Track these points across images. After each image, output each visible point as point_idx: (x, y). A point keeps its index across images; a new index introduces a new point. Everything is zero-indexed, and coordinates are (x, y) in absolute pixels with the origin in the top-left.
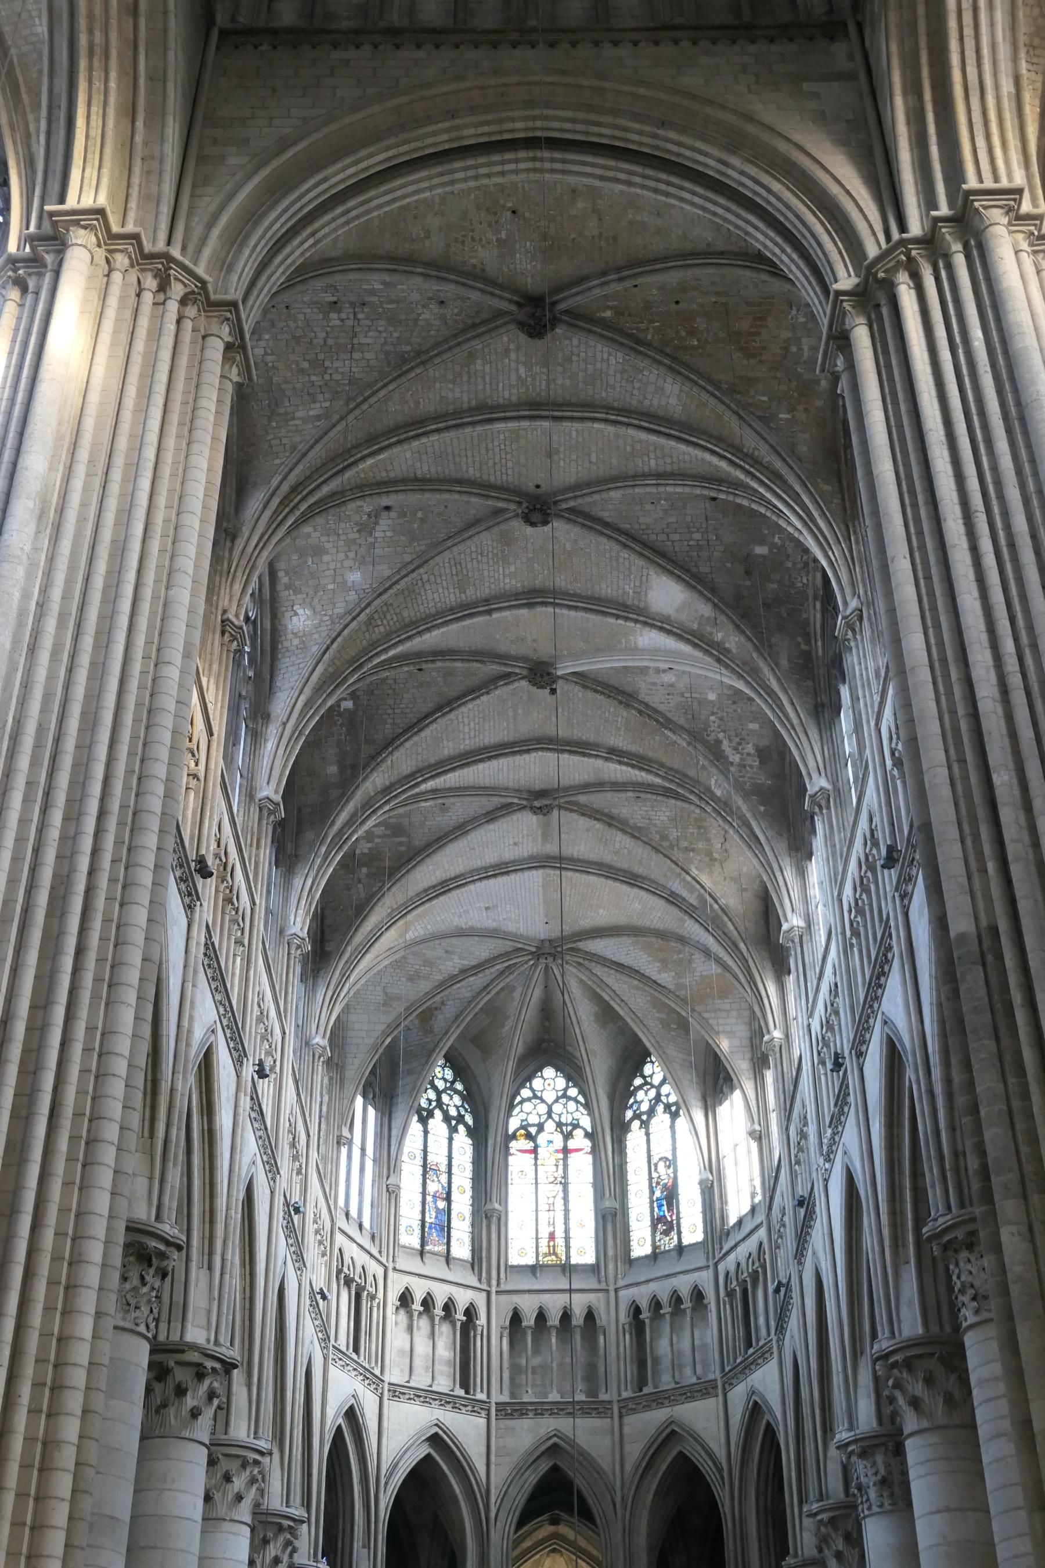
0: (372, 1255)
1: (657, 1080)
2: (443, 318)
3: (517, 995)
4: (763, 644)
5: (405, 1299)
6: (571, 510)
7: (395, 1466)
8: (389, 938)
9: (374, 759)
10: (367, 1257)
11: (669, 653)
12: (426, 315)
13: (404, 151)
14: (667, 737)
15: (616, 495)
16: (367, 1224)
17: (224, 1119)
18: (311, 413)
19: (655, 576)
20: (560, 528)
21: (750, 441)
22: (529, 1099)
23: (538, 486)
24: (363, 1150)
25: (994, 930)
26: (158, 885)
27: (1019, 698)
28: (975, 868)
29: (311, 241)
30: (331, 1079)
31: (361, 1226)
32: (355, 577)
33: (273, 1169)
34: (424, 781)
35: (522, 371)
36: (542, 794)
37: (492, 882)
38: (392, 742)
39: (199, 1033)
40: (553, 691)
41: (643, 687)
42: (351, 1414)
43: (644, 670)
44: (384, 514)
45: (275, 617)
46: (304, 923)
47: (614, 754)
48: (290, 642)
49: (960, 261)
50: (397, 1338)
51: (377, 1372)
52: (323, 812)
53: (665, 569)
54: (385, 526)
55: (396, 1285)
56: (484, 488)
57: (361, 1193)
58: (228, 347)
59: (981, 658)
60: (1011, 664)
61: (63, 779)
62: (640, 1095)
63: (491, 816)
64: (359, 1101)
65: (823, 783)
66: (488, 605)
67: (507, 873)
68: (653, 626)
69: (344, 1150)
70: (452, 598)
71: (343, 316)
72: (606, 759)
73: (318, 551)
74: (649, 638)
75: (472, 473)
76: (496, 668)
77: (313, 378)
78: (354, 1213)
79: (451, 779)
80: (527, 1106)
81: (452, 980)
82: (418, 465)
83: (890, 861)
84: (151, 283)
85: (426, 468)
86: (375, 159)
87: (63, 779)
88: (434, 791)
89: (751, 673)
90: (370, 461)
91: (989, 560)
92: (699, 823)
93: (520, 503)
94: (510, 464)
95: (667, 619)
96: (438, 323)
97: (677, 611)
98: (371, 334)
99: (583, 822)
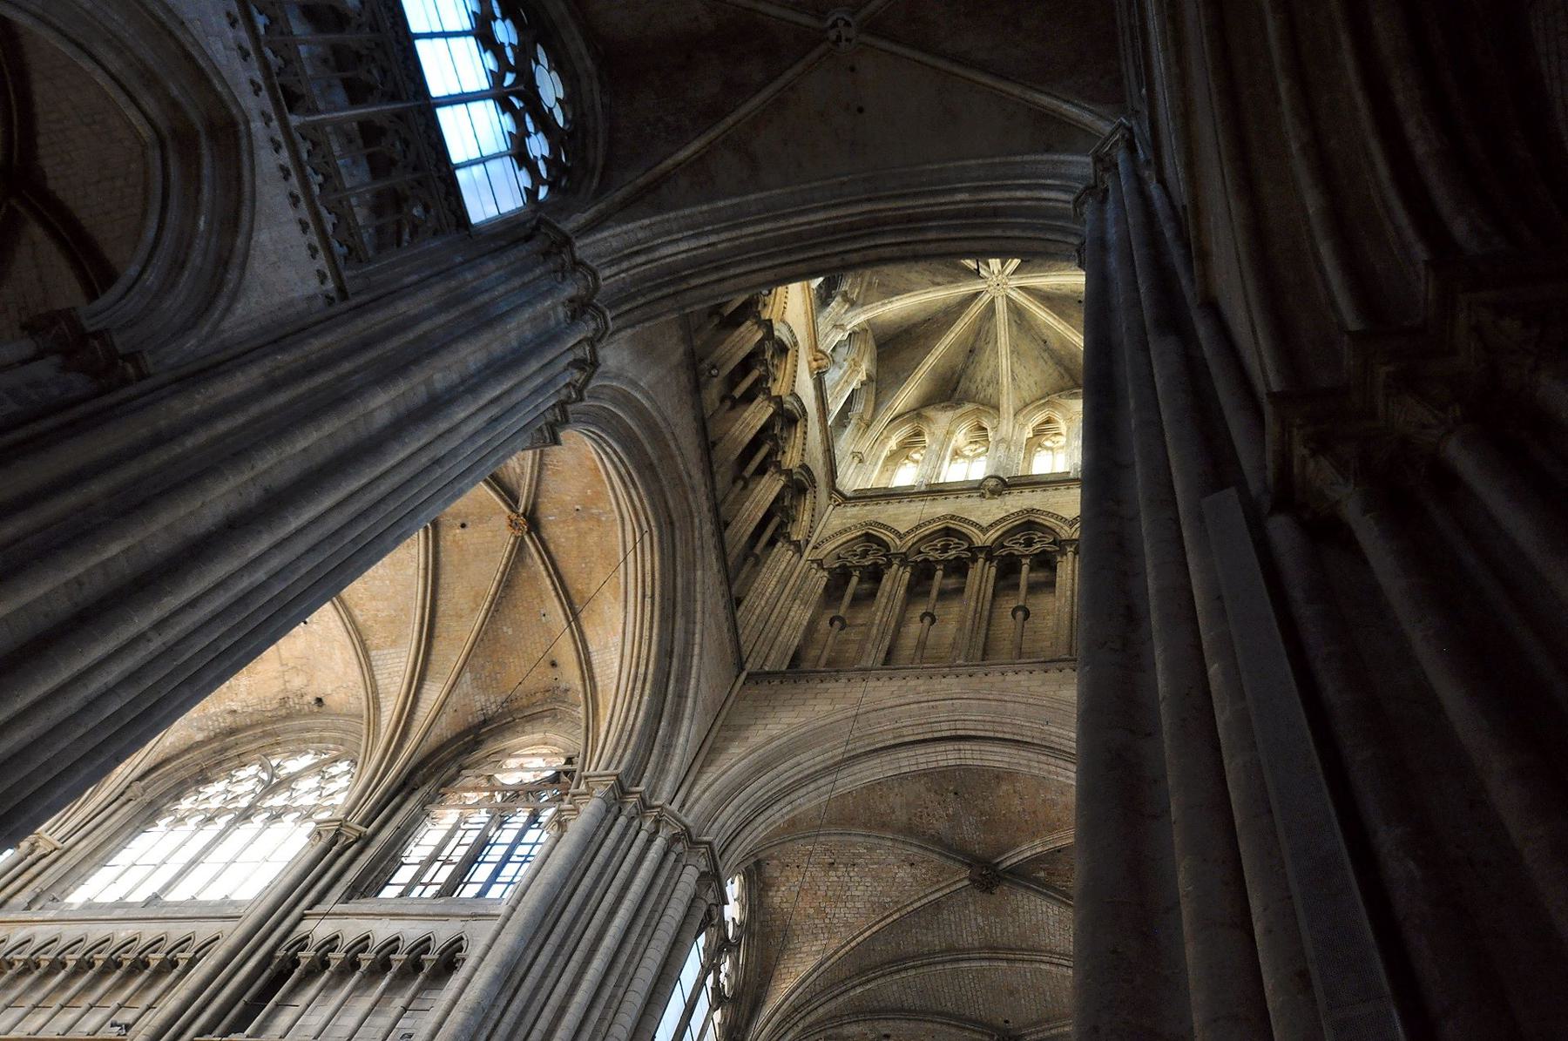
2: (914, 877)
12: (901, 874)
18: (814, 949)
23: (1007, 1022)
29: (789, 808)
35: (980, 919)
58: (703, 875)
71: (839, 874)
77: (816, 921)
82: (904, 997)
90: (859, 990)
94: (980, 1001)
96: (911, 880)
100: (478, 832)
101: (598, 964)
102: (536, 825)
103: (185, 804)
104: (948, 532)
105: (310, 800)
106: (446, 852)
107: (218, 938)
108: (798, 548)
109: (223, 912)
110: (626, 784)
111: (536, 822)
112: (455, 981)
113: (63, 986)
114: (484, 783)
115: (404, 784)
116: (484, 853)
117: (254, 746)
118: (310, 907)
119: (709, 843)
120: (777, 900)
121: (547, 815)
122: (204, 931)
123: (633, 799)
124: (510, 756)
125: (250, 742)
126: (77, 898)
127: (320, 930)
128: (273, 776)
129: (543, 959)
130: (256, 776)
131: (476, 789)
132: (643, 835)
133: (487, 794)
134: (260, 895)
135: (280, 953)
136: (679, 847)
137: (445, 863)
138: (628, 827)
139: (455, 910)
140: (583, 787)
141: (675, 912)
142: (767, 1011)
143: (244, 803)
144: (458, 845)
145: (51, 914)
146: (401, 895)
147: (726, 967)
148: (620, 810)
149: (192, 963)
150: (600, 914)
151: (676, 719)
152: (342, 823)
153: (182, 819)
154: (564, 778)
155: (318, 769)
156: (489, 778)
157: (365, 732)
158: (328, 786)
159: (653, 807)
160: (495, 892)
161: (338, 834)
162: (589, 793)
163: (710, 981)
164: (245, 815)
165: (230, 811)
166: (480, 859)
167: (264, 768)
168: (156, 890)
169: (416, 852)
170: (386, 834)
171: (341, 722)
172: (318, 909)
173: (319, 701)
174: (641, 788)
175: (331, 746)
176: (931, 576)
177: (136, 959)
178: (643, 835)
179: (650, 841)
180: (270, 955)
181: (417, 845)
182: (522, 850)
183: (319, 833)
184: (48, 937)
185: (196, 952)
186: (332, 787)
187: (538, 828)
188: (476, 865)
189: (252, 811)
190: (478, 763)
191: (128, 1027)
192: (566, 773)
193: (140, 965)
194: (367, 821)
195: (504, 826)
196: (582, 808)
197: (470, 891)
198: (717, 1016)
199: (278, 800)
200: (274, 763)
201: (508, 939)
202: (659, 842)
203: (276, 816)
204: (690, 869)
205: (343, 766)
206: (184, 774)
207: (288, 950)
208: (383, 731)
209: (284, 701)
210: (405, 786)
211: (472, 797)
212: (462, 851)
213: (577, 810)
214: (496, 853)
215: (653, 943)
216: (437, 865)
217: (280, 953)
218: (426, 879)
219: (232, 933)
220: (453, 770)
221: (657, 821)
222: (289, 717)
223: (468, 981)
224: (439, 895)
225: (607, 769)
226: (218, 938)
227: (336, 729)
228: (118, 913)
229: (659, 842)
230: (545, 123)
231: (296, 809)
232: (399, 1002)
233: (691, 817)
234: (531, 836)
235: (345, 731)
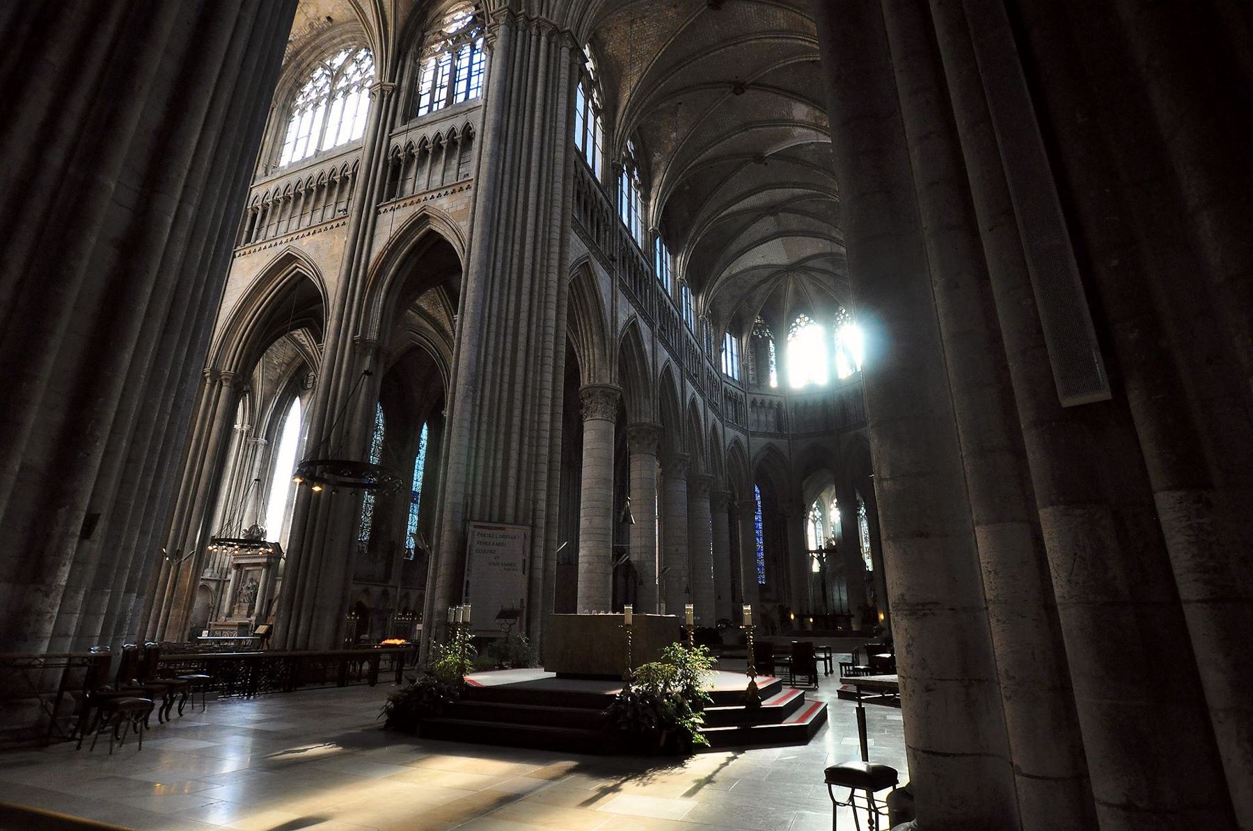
0: (739, 389)
1: (844, 311)
2: (678, 13)
3: (783, 288)
5: (754, 403)
6: (752, 84)
7: (755, 459)
8: (725, 274)
10: (737, 390)
14: (816, 173)
16: (736, 378)
17: (648, 347)
19: (793, 104)
20: (749, 93)
22: (795, 326)
23: (737, 77)
24: (732, 353)
30: (715, 331)
31: (734, 379)
33: (680, 364)
34: (723, 212)
36: (772, 207)
37: (761, 246)
39: (622, 318)
40: (766, 164)
42: (736, 442)
44: (679, 106)
46: (683, 274)
47: (796, 185)
50: (752, 416)
51: (746, 428)
53: (800, 101)
55: (750, 398)
57: (732, 367)
58: (571, 50)
62: (838, 319)
63: (754, 221)
64: (728, 335)
67: (766, 242)
68: (797, 126)
69: (723, 354)
72: (793, 188)
74: (798, 131)
78: (730, 375)
79: (734, 208)
80: (794, 329)
81: (755, 287)
88: (728, 215)
93: (731, 87)
95: (802, 121)
96: (676, 16)
97: (807, 116)
98: (651, 29)
99: (791, 216)
100: (449, 65)
101: (538, 114)
102: (476, 52)
103: (300, 101)
105: (357, 78)
106: (439, 82)
107: (358, 160)
109: (353, 148)
110: (514, 11)
111: (475, 49)
112: (476, 144)
113: (306, 203)
114: (440, 38)
115: (399, 52)
116: (457, 76)
117: (312, 57)
118: (391, 132)
119: (569, 31)
120: (610, 51)
121: (480, 43)
122: (351, 161)
123: (521, 19)
124: (445, 15)
125: (309, 56)
126: (284, 162)
128: (331, 71)
129: (512, 121)
130: (323, 73)
131: (437, 41)
132: (534, 38)
133: (443, 42)
134: (364, 134)
135: (390, 158)
136: (554, 39)
137: (441, 87)
138: (524, 36)
139: (458, 110)
140: (492, 21)
141: (564, 74)
142: (621, 109)
143: (327, 90)
144: (443, 76)
145: (278, 175)
146: (429, 111)
147: (595, 95)
148: (517, 28)
149: (354, 175)
150: (529, 89)
152: (381, 84)
153: (304, 109)
154: (479, 19)
155: (351, 58)
156: (440, 32)
157: (364, 29)
158: (362, 66)
159: (533, 20)
160: (472, 95)
161: (382, 91)
162: (497, 24)
163: (590, 105)
164: (332, 97)
165: (323, 97)
166: (457, 80)
167: (324, 68)
168: (315, 147)
169: (425, 87)
170: (405, 83)
171: (347, 27)
172: (395, 131)
173: (329, 18)
174: (523, 11)
175: (350, 43)
177: (329, 181)
178: (534, 38)
179: (538, 40)
181: (423, 83)
182: (475, 68)
183: (373, 94)
184: (286, 184)
185: (353, 170)
187: (478, 52)
188: (456, 84)
189: (333, 93)
190: (430, 26)
191: (346, 210)
192: (478, 15)
193: (332, 184)
194: (392, 79)
195: (461, 57)
196: (497, 34)
197: (461, 98)
198: (599, 120)
199: (342, 83)
200: (328, 63)
201: (491, 116)
202: (543, 39)
203: (347, 92)
204: (564, 49)
205: (363, 53)
206: (288, 85)
207: (392, 155)
208: (372, 25)
209: (311, 25)
210: (400, 55)
211: (437, 47)
212: (446, 78)
213: (494, 35)
214: (463, 74)
215: (560, 95)
216: (438, 90)
217: (390, 158)
218: (436, 100)
219: (364, 157)
220: (419, 35)
221: (538, 28)
222: (319, 34)
223: (482, 142)
224: (446, 105)
225: (500, 6)
226: (358, 160)
227: (347, 32)
228: (307, 164)
231: (354, 85)
232: (455, 162)
233: (555, 19)
234: (476, 58)
235: (352, 32)
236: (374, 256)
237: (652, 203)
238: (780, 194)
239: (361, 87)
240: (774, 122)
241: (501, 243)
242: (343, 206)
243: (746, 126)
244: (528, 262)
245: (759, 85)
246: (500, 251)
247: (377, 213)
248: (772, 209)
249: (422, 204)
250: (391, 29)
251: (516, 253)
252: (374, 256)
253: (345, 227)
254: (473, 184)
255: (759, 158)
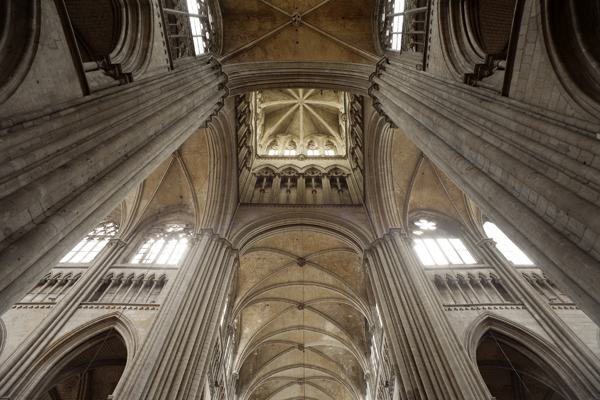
4: (352, 338)
9: (261, 368)
11: (332, 342)
13: (274, 225)
15: (318, 303)
21: (348, 289)
25: (417, 390)
26: (203, 377)
27: (415, 330)
28: (409, 374)
32: (260, 321)
36: (300, 379)
38: (265, 364)
41: (324, 351)
43: (324, 346)
45: (241, 330)
47: (318, 368)
48: (243, 336)
49: (390, 242)
52: (248, 381)
54: (267, 309)
56: (289, 301)
59: (404, 321)
60: (412, 323)
61: (183, 345)
63: (288, 385)
65: (368, 371)
66: (291, 328)
70: (281, 327)
73: (252, 315)
74: (326, 338)
75: (286, 297)
76: (291, 345)
83: (387, 385)
84: (220, 244)
85: (277, 296)
86: (269, 226)
87: (183, 345)
89: (349, 345)
91: (404, 300)
92: (339, 387)
99: (310, 387)
104: (290, 168)
105: (102, 234)
108: (249, 169)
112: (165, 287)
122: (75, 272)
127: (117, 272)
151: (225, 214)
176: (262, 181)
180: (101, 279)
186: (109, 230)
202: (224, 249)
205: (111, 224)
210: (136, 231)
229: (224, 249)
230: (209, 30)
236: (61, 334)
237: (238, 356)
238: (309, 372)
239: (102, 238)
240: (314, 329)
241: (171, 348)
242: (52, 296)
243: (300, 327)
244: (184, 366)
245: (310, 308)
246: (169, 353)
247: (79, 307)
248: (301, 381)
249: (116, 310)
250: (137, 219)
251: (178, 359)
252: (61, 334)
253: (48, 310)
254: (159, 308)
255: (301, 347)
